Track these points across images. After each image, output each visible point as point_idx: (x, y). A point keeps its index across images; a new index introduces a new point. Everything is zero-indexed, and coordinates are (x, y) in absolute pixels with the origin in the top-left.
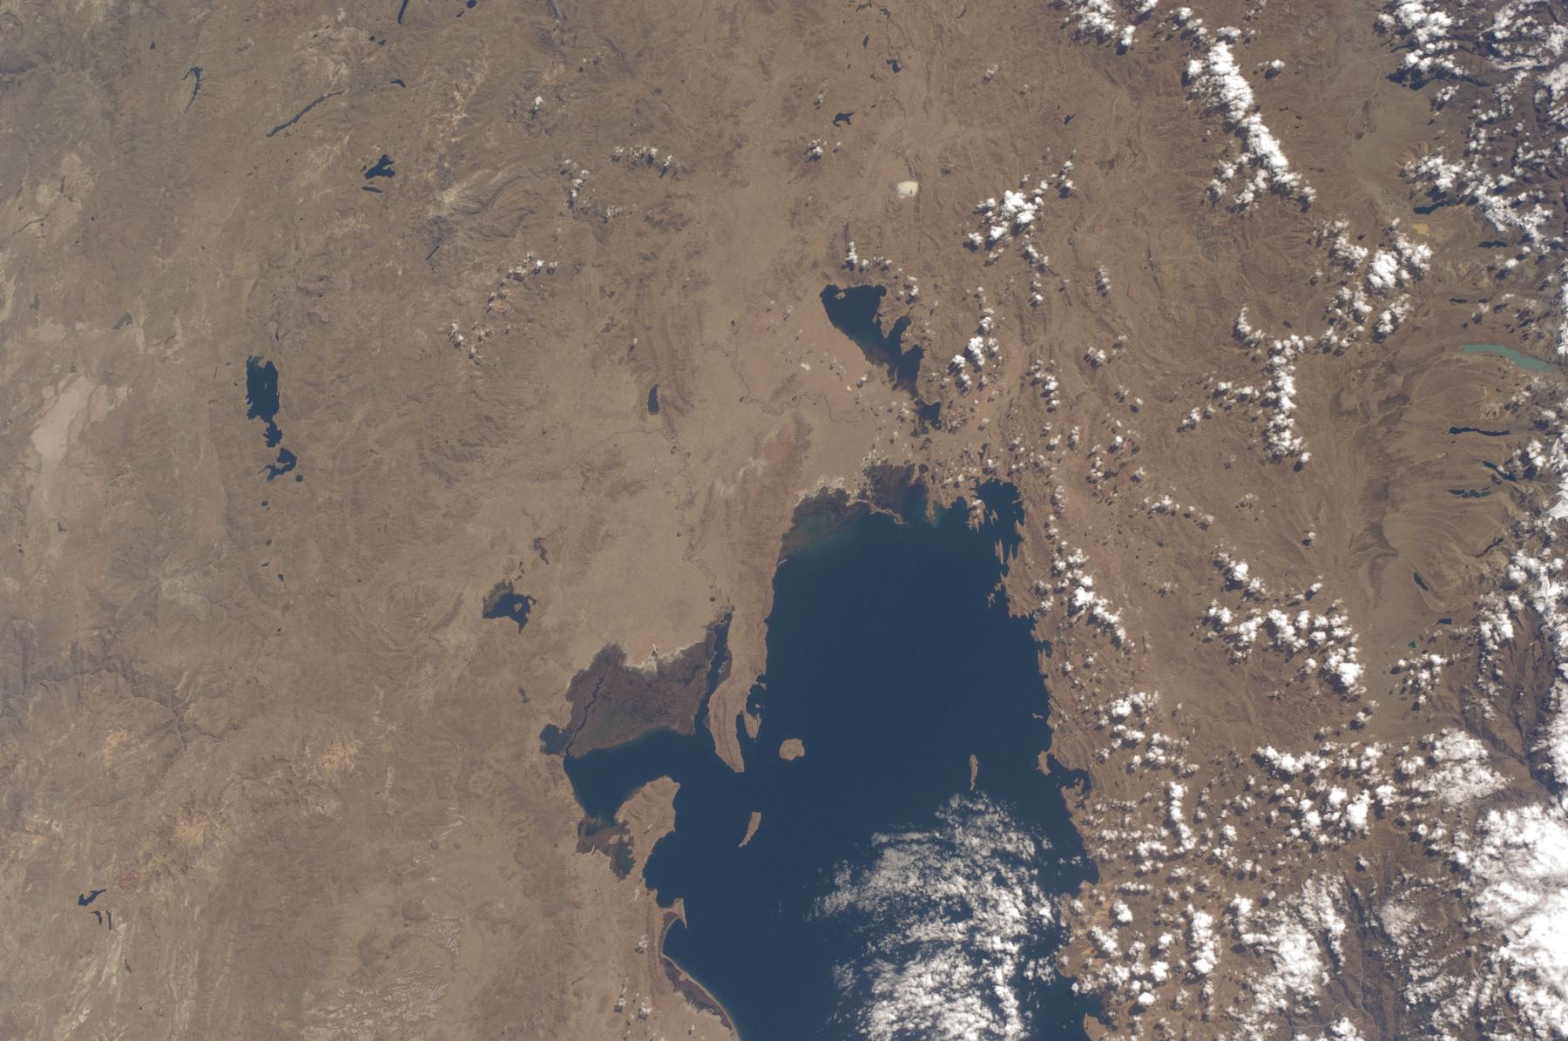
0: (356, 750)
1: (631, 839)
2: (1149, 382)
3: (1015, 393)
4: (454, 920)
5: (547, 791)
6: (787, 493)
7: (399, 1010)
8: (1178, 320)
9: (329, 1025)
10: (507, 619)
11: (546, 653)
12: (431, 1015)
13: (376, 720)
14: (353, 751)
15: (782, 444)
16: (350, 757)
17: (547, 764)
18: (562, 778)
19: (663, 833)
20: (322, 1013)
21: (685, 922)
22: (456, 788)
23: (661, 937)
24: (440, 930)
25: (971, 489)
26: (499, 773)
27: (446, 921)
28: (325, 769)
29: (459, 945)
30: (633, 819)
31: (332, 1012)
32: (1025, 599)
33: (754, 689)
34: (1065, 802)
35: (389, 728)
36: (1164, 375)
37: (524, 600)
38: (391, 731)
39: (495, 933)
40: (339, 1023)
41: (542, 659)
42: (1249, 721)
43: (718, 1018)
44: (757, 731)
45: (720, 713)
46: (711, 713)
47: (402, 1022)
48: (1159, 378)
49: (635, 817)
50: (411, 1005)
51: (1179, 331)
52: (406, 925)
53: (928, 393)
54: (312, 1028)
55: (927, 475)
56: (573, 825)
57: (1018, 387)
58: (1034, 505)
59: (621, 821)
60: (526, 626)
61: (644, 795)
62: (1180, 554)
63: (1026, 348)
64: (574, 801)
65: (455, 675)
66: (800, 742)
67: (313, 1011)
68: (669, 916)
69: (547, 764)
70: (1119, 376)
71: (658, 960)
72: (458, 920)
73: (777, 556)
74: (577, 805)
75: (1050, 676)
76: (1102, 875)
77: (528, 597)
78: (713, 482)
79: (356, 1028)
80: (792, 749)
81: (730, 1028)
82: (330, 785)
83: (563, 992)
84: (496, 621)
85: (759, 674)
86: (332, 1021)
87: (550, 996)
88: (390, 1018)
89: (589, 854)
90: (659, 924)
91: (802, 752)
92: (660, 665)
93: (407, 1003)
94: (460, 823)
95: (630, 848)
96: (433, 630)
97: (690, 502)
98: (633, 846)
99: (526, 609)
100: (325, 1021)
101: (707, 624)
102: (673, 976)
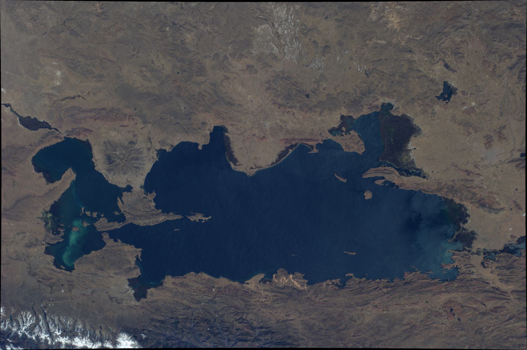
0: (396, 28)
1: (343, 135)
2: (484, 328)
3: (492, 285)
4: (321, 66)
5: (367, 105)
6: (471, 203)
7: (289, 44)
8: (507, 341)
9: (286, 16)
10: (442, 91)
11: (424, 107)
12: (286, 57)
13: (407, 36)
14: (396, 26)
15: (493, 203)
16: (393, 26)
17: (378, 105)
18: (371, 111)
19: (344, 147)
20: (291, 13)
21: (310, 153)
22: (374, 69)
23: (305, 144)
24: (318, 61)
25: (457, 266)
26: (377, 86)
27: (321, 64)
28: (390, 14)
29: (312, 68)
30: (351, 137)
31: (291, 17)
32: (410, 277)
33: (394, 184)
34: (335, 279)
35: (403, 42)
36: (486, 333)
37: (449, 99)
38: (402, 43)
39: (314, 82)
40: (286, 20)
41: (422, 104)
42: (353, 336)
43: (275, 161)
44: (378, 183)
45: (386, 171)
46: (387, 168)
47: (285, 45)
48: (485, 331)
49: (351, 138)
50: (291, 49)
51: (502, 340)
52: (321, 47)
53: (501, 257)
54: (286, 9)
55: (466, 252)
56: (352, 114)
57: (494, 286)
58: (445, 285)
59: (351, 132)
60: (437, 99)
61: (359, 141)
62: (416, 327)
63: (510, 291)
64: (361, 115)
65: (421, 69)
66: (370, 198)
67: (292, 9)
68: (312, 147)
69: (378, 105)
70: (489, 319)
71: (297, 142)
72: (321, 68)
73: (445, 197)
74: (359, 116)
75: (380, 281)
76: (309, 286)
77: (449, 100)
78: (482, 176)
79: (284, 27)
80: (368, 195)
81: (271, 165)
82: (383, 16)
83: (289, 107)
84: (442, 87)
85: (399, 186)
86: (288, 17)
87: (288, 103)
88: (287, 41)
89: (339, 119)
90: (311, 143)
91: (366, 198)
92: (410, 150)
93: (292, 47)
94: (359, 70)
95: (340, 135)
96: (443, 60)
97: (476, 166)
98: (340, 136)
99: (445, 99)
100: (288, 14)
101: (423, 169)
102: (292, 147)
